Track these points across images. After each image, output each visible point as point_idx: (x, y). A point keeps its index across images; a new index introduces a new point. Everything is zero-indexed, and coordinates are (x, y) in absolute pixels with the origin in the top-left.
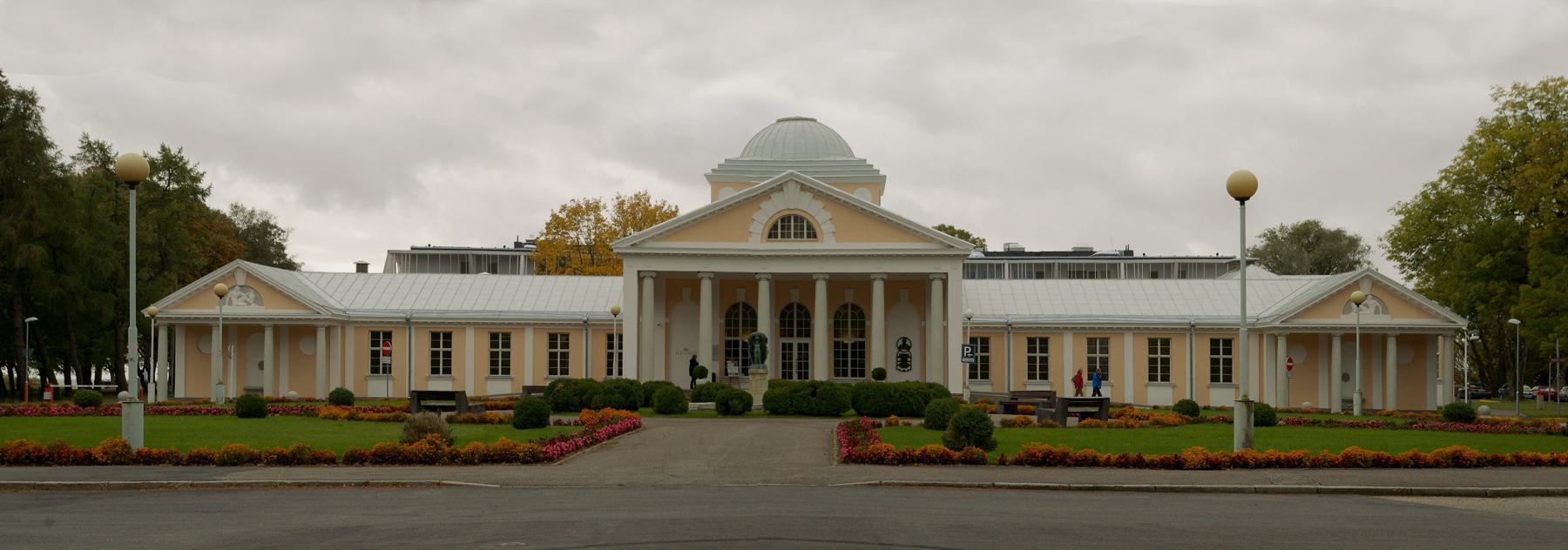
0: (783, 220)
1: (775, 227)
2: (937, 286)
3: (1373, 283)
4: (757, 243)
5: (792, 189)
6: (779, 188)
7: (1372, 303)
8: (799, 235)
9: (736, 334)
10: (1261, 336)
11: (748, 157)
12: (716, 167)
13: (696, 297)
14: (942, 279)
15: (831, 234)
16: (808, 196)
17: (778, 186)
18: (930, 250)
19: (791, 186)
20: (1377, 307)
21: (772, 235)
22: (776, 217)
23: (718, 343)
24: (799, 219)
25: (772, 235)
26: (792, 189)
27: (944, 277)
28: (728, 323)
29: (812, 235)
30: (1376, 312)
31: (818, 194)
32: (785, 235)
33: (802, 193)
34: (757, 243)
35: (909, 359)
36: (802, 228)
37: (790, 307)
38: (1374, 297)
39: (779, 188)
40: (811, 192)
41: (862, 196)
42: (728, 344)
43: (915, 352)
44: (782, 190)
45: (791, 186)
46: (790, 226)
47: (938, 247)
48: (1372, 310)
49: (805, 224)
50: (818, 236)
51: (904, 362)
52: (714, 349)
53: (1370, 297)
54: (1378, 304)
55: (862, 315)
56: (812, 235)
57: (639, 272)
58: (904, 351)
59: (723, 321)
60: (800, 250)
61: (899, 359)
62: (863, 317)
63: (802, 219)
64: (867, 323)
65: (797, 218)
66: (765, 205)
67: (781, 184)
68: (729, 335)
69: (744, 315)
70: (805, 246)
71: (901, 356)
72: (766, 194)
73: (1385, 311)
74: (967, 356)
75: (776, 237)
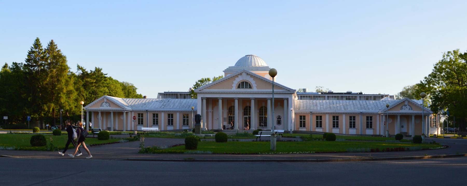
1: (240, 85)
2: (285, 101)
3: (408, 102)
4: (234, 89)
5: (244, 74)
6: (241, 74)
7: (408, 107)
8: (246, 87)
14: (287, 100)
18: (283, 91)
19: (244, 74)
20: (409, 108)
21: (239, 87)
22: (239, 83)
24: (246, 83)
25: (239, 87)
26: (244, 74)
27: (287, 99)
29: (250, 87)
30: (409, 109)
32: (243, 87)
34: (234, 89)
36: (247, 85)
38: (409, 105)
39: (241, 74)
40: (250, 75)
44: (241, 74)
45: (244, 74)
46: (244, 85)
48: (408, 109)
49: (248, 84)
50: (252, 87)
53: (408, 105)
54: (410, 107)
56: (250, 87)
57: (202, 98)
60: (246, 91)
63: (247, 83)
66: (237, 79)
67: (241, 73)
70: (248, 90)
72: (237, 76)
73: (412, 109)
75: (240, 87)
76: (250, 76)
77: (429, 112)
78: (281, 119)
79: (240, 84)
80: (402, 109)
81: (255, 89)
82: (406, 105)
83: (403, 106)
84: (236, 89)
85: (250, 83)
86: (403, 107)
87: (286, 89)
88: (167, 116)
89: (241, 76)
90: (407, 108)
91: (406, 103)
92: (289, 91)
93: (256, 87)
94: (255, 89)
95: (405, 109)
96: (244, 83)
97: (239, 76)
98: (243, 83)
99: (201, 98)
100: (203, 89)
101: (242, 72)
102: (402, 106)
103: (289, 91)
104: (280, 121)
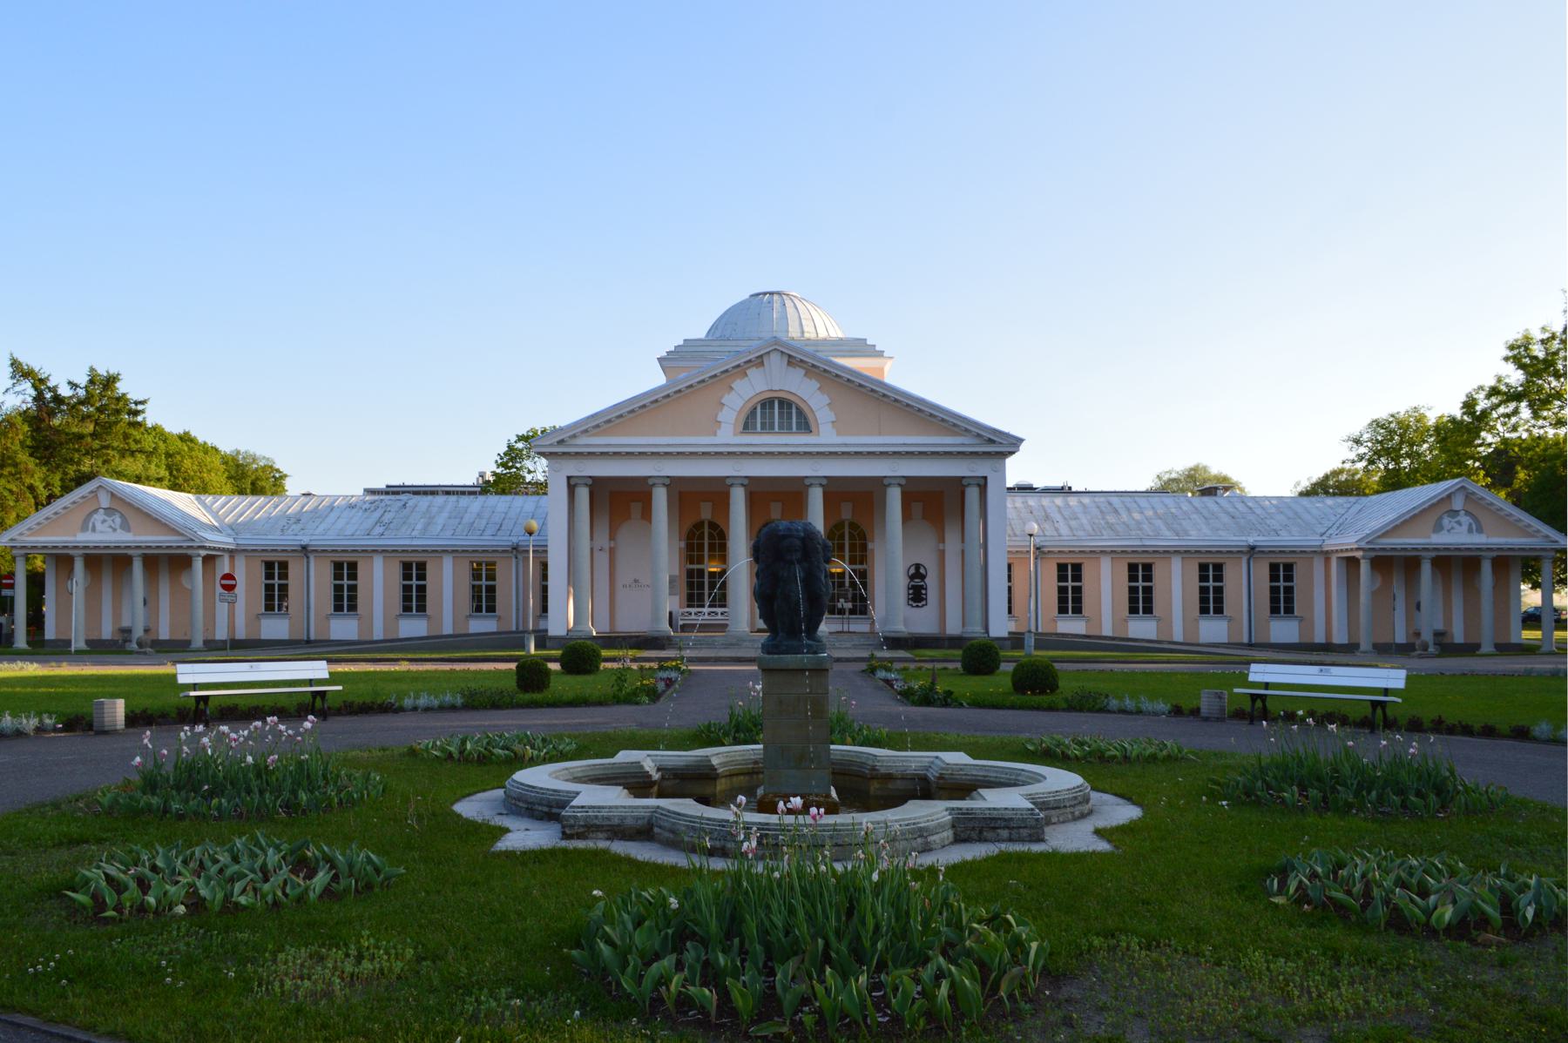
1: (753, 412)
2: (972, 494)
3: (1467, 497)
4: (727, 435)
6: (759, 361)
7: (1465, 520)
8: (786, 428)
9: (700, 561)
10: (1327, 561)
14: (979, 485)
15: (830, 425)
16: (798, 373)
17: (757, 357)
19: (775, 357)
20: (1470, 525)
21: (748, 426)
22: (750, 405)
23: (676, 572)
24: (785, 404)
25: (748, 426)
26: (775, 362)
27: (982, 482)
28: (690, 547)
29: (805, 426)
30: (1470, 530)
32: (768, 427)
33: (791, 369)
34: (727, 435)
35: (924, 592)
38: (1468, 513)
39: (759, 361)
40: (804, 368)
42: (690, 574)
43: (931, 582)
44: (762, 364)
45: (775, 357)
48: (1465, 528)
49: (794, 411)
50: (813, 428)
51: (917, 595)
52: (672, 581)
53: (1462, 513)
54: (1471, 521)
55: (863, 537)
56: (805, 426)
58: (917, 582)
59: (683, 544)
60: (786, 445)
61: (911, 592)
62: (865, 538)
65: (782, 402)
67: (761, 356)
68: (692, 563)
69: (711, 537)
71: (913, 587)
72: (740, 370)
73: (1480, 530)
76: (803, 372)
77: (1557, 542)
78: (926, 580)
79: (755, 408)
80: (1438, 528)
81: (826, 435)
82: (1456, 512)
83: (1445, 516)
84: (735, 434)
85: (802, 405)
86: (1446, 521)
87: (979, 435)
88: (397, 571)
89: (761, 369)
90: (1459, 523)
91: (1458, 503)
92: (991, 441)
93: (833, 422)
94: (826, 435)
95: (1452, 528)
96: (772, 407)
97: (753, 373)
98: (767, 404)
99: (565, 480)
100: (574, 436)
101: (769, 353)
102: (1440, 518)
103: (991, 441)
104: (922, 587)
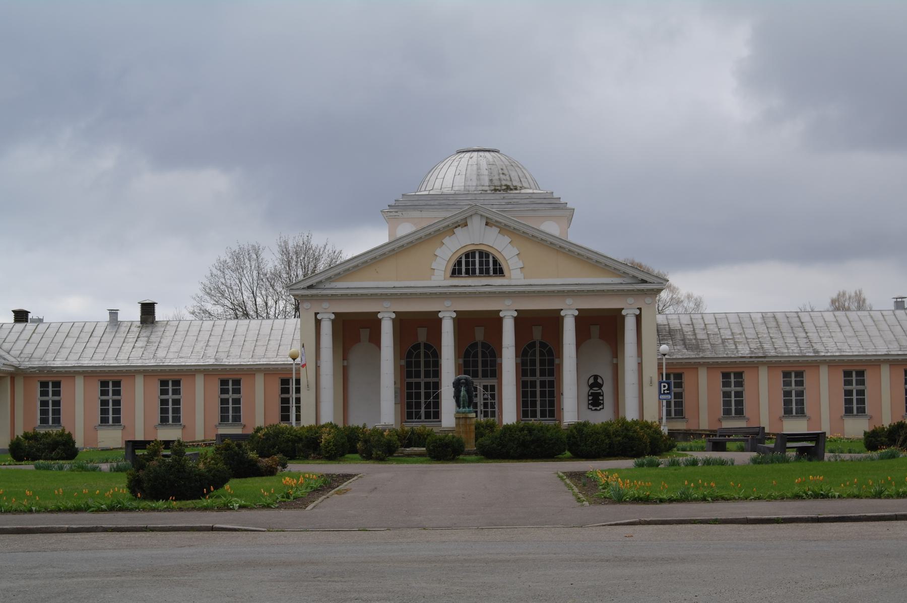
0: (467, 255)
1: (459, 263)
5: (476, 224)
8: (485, 272)
11: (425, 190)
12: (393, 203)
13: (376, 339)
15: (519, 269)
16: (494, 231)
21: (456, 272)
25: (456, 272)
26: (476, 224)
29: (499, 271)
31: (505, 229)
32: (470, 273)
37: (417, 347)
41: (551, 228)
43: (607, 390)
44: (466, 225)
47: (628, 280)
55: (550, 353)
56: (499, 271)
61: (590, 398)
63: (487, 255)
64: (557, 361)
65: (481, 253)
72: (450, 229)
74: (664, 393)
100: (321, 282)
